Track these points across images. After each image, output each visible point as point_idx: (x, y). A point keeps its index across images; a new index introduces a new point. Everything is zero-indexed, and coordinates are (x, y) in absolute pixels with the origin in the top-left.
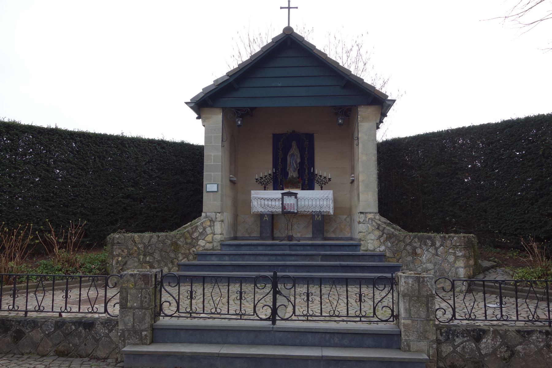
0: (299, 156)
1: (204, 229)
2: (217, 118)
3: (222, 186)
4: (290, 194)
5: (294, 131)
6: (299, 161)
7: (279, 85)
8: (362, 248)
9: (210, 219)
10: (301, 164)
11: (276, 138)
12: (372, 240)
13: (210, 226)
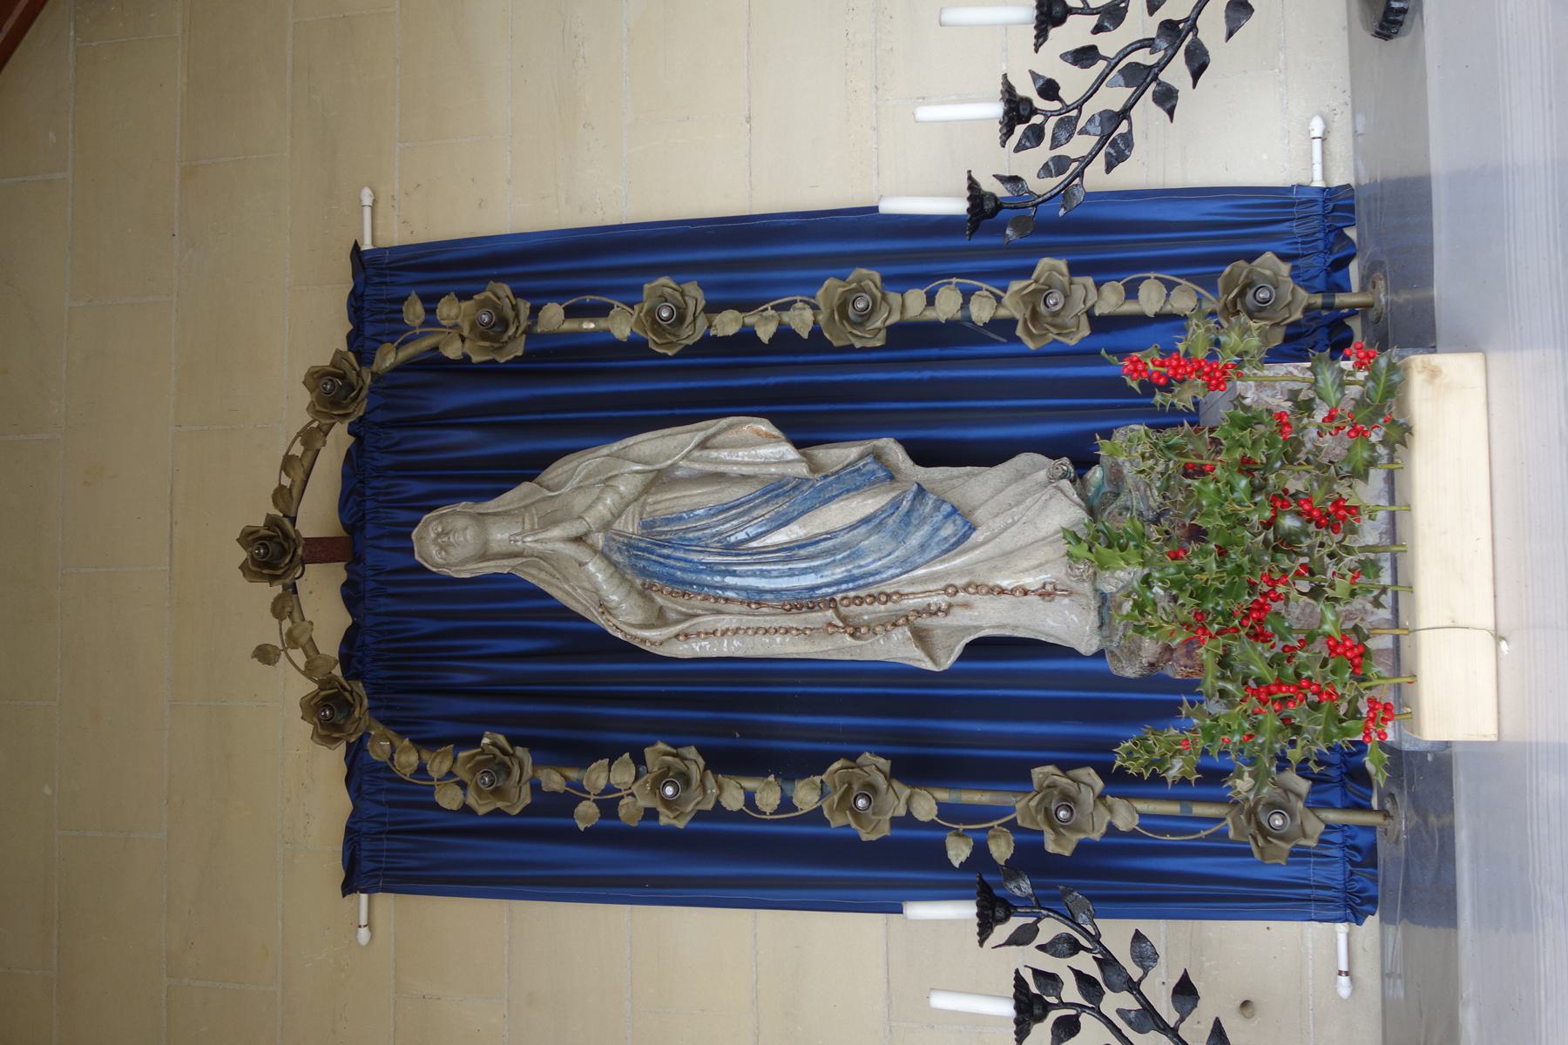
5: (273, 552)
6: (757, 447)
10: (812, 397)
11: (394, 847)
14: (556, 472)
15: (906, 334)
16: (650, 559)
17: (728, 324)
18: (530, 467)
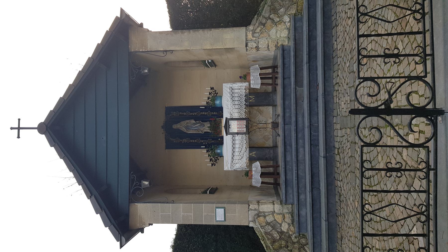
0: (188, 121)
1: (268, 224)
2: (141, 209)
3: (218, 203)
4: (227, 127)
5: (163, 127)
7: (105, 138)
8: (286, 43)
9: (256, 216)
10: (196, 119)
11: (170, 145)
12: (277, 32)
13: (265, 217)
14: (181, 122)
15: (202, 115)
16: (187, 128)
17: (191, 114)
18: (179, 122)
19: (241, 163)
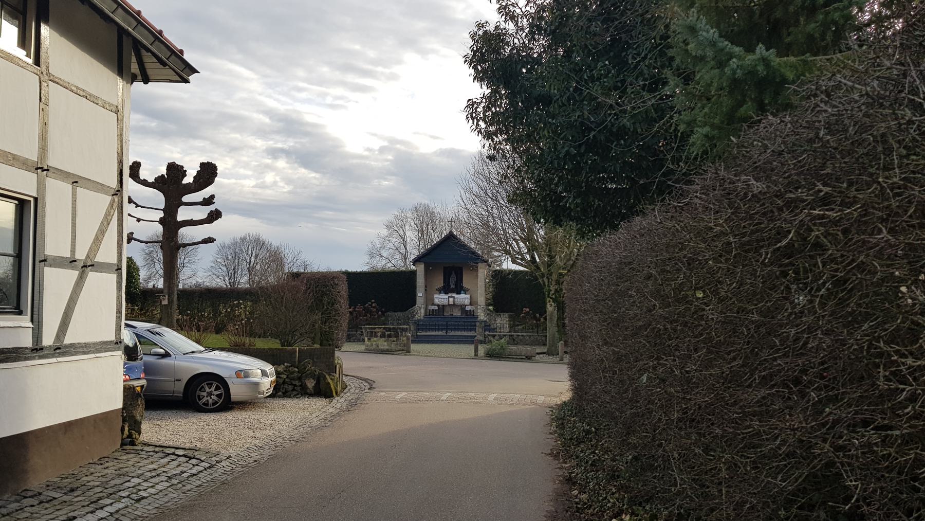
19: (437, 301)
